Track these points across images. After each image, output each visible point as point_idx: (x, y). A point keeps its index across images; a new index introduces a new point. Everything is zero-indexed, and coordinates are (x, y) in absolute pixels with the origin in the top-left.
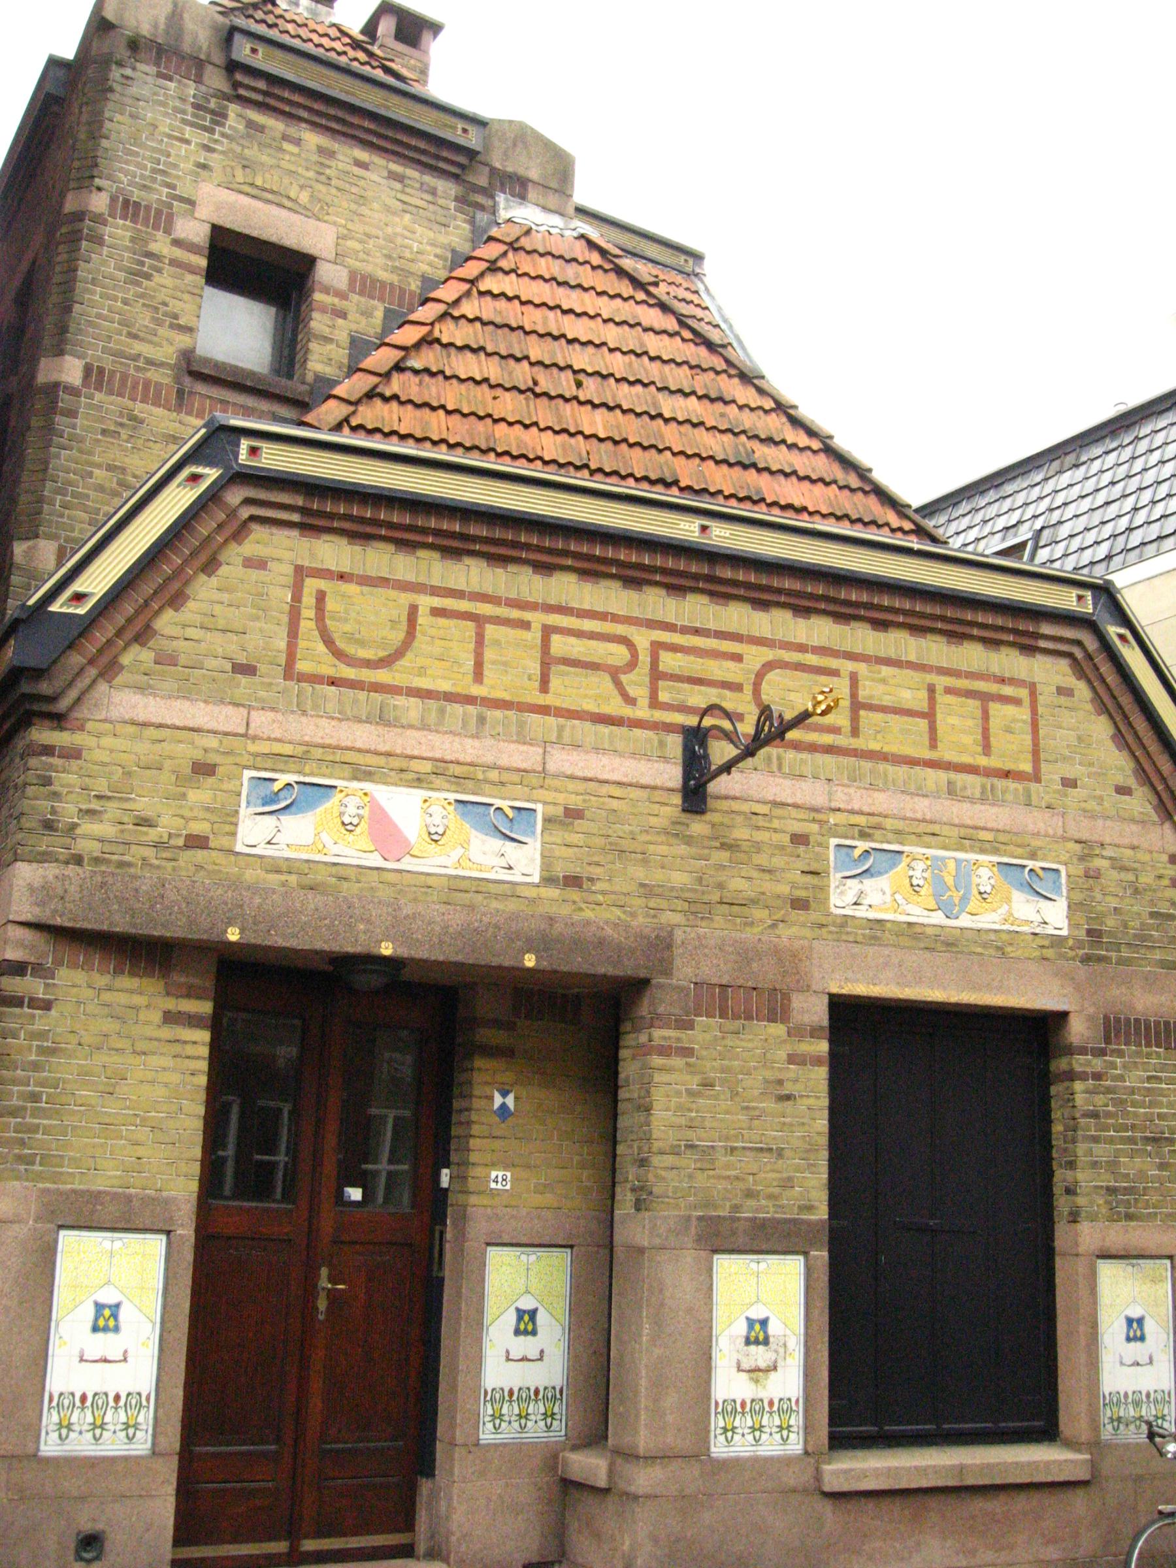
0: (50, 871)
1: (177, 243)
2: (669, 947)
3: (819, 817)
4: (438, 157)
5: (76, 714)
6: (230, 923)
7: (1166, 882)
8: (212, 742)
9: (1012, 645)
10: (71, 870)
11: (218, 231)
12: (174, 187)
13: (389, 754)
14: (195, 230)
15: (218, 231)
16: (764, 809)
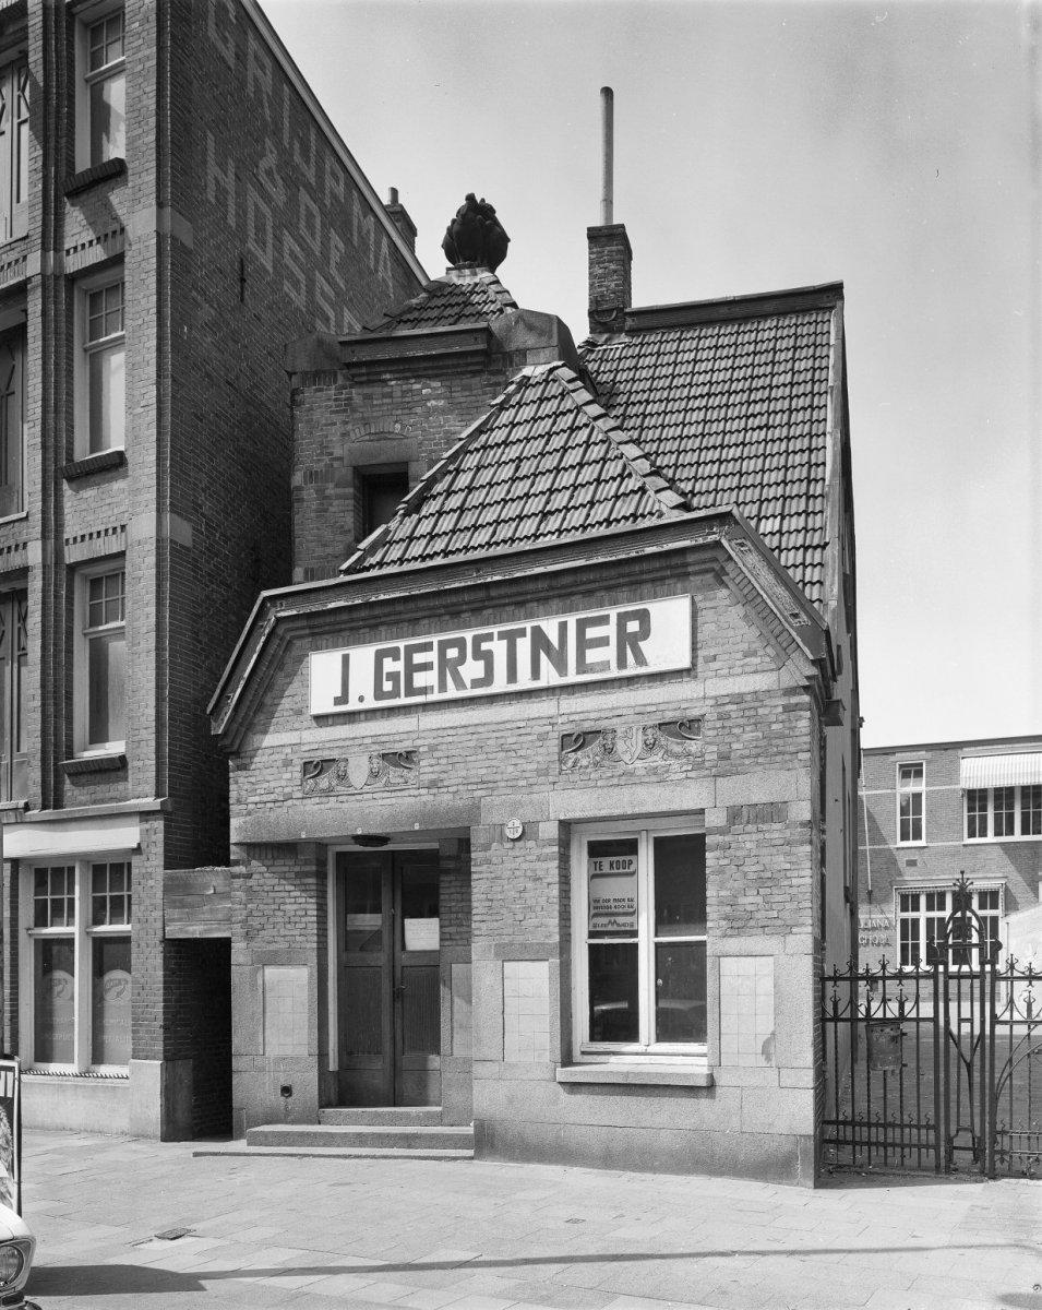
0: (242, 819)
1: (337, 486)
2: (479, 808)
3: (552, 721)
4: (468, 365)
5: (246, 748)
6: (302, 829)
7: (780, 709)
8: (289, 750)
9: (672, 576)
10: (248, 818)
11: (357, 470)
12: (332, 454)
13: (353, 739)
14: (345, 472)
15: (357, 470)
16: (522, 724)
